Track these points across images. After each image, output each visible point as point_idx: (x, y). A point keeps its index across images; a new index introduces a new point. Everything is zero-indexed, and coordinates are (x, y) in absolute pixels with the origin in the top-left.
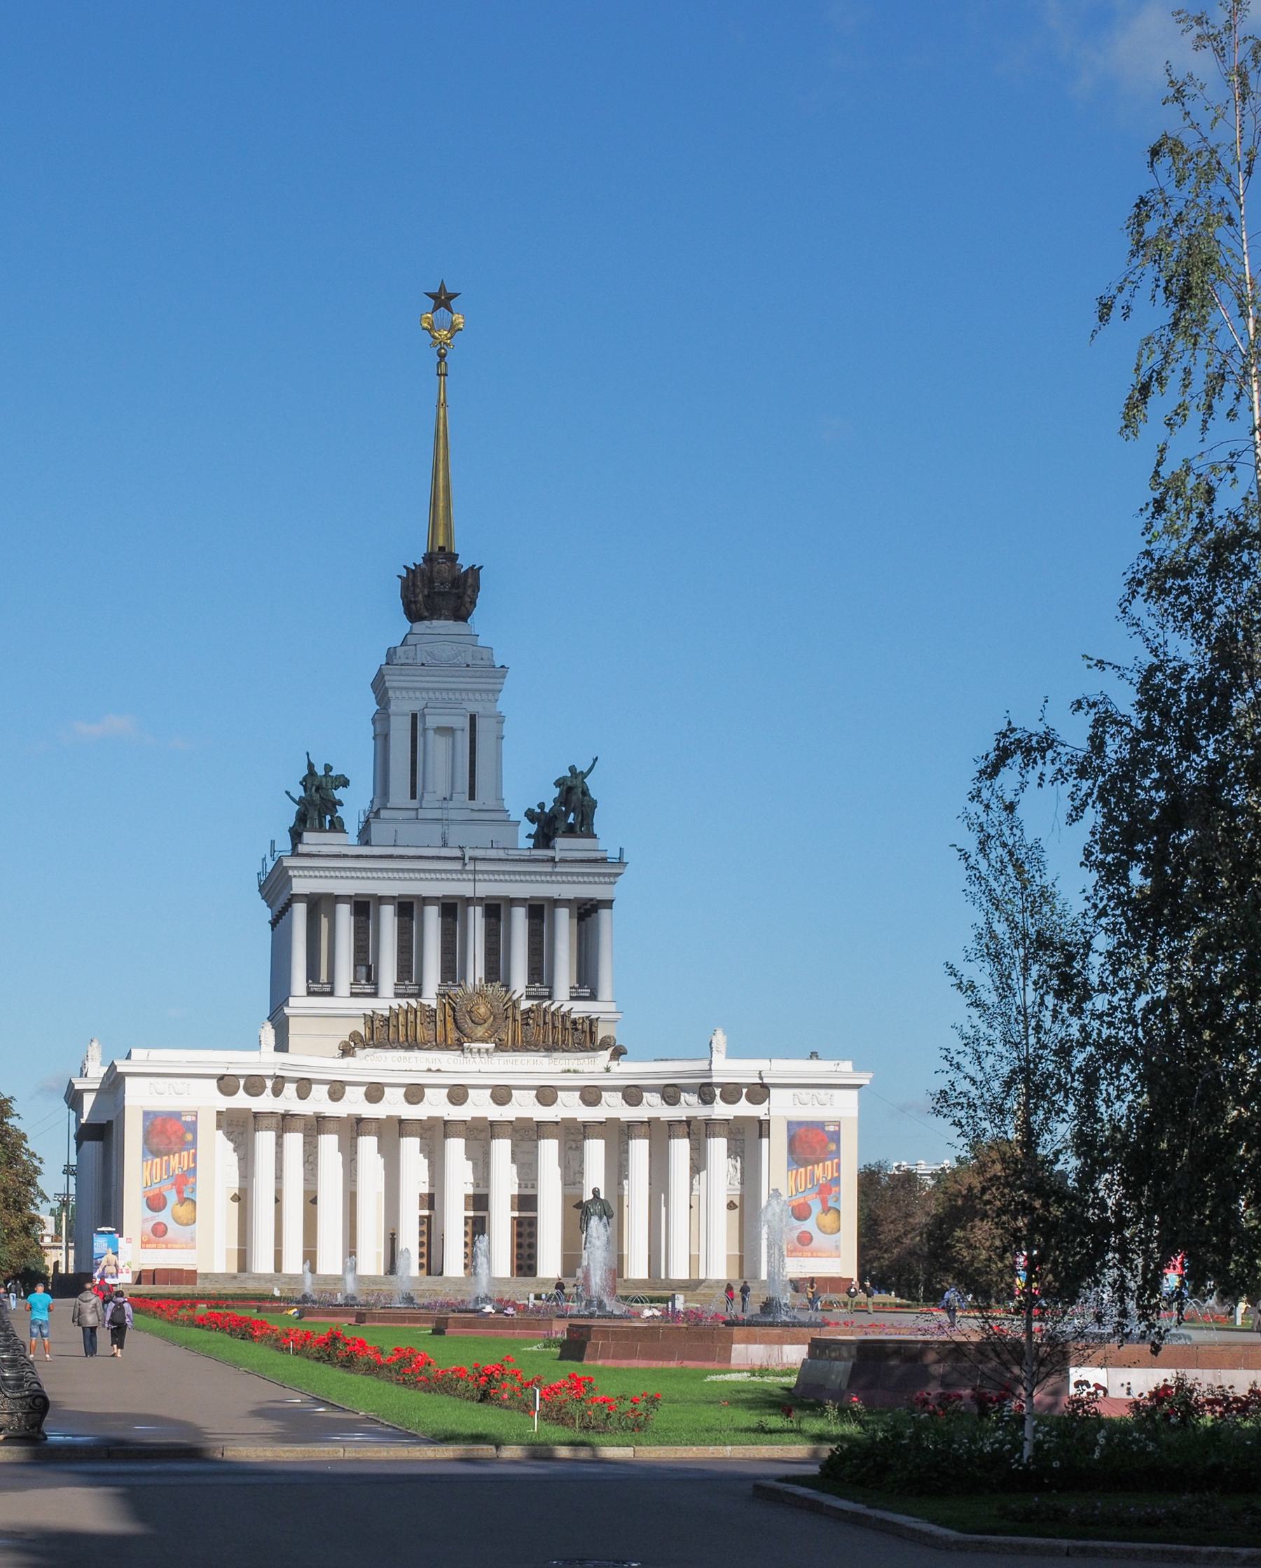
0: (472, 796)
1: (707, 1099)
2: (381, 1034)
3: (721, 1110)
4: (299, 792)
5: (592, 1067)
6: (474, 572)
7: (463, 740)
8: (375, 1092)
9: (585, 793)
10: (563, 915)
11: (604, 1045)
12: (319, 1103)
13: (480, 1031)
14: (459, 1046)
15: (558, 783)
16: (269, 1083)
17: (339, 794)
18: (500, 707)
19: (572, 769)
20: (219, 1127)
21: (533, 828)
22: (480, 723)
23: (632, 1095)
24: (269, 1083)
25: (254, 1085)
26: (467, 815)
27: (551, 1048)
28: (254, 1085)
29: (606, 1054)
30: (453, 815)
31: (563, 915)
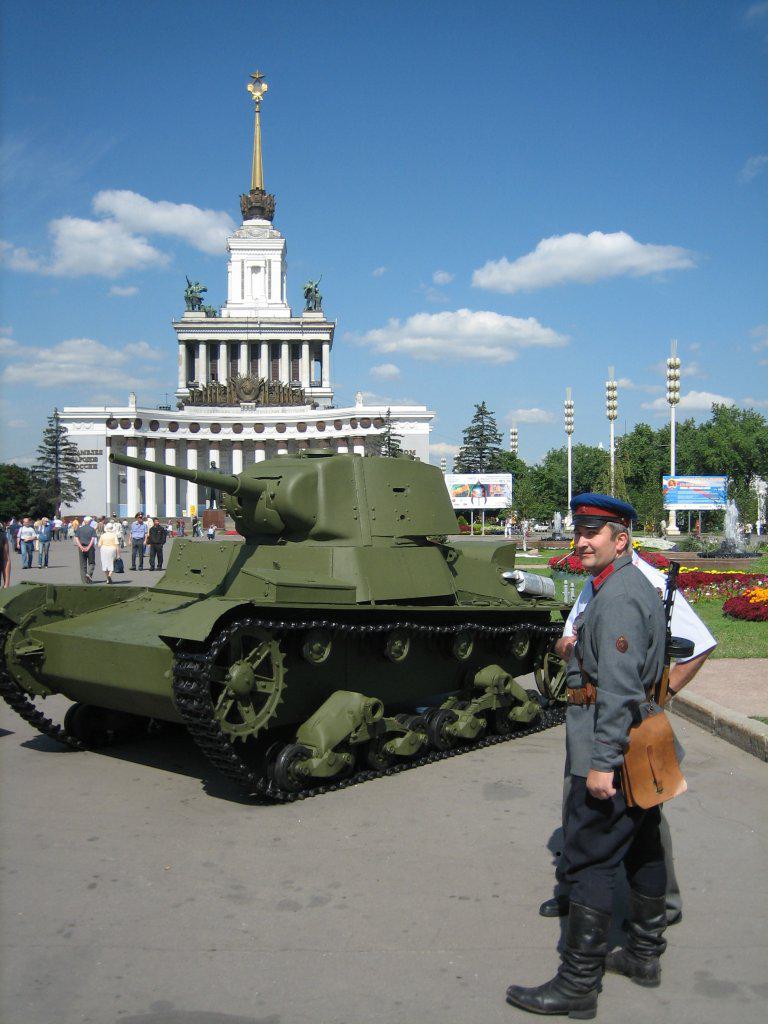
0: (270, 297)
1: (354, 427)
2: (197, 399)
3: (361, 431)
5: (303, 413)
6: (271, 198)
8: (195, 428)
11: (308, 403)
12: (163, 433)
13: (248, 397)
14: (237, 404)
16: (132, 423)
17: (201, 295)
23: (321, 426)
24: (132, 423)
25: (125, 424)
27: (283, 404)
28: (125, 424)
29: (309, 406)
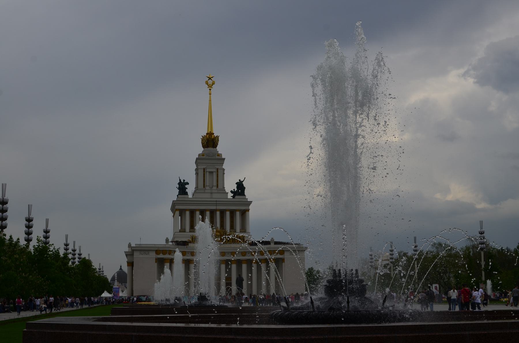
0: (217, 187)
4: (178, 186)
6: (218, 137)
7: (215, 175)
9: (243, 185)
10: (238, 213)
15: (236, 183)
17: (187, 186)
18: (224, 167)
19: (240, 180)
20: (156, 262)
21: (232, 195)
22: (219, 171)
26: (216, 191)
28: (164, 252)
30: (213, 191)
31: (238, 213)
